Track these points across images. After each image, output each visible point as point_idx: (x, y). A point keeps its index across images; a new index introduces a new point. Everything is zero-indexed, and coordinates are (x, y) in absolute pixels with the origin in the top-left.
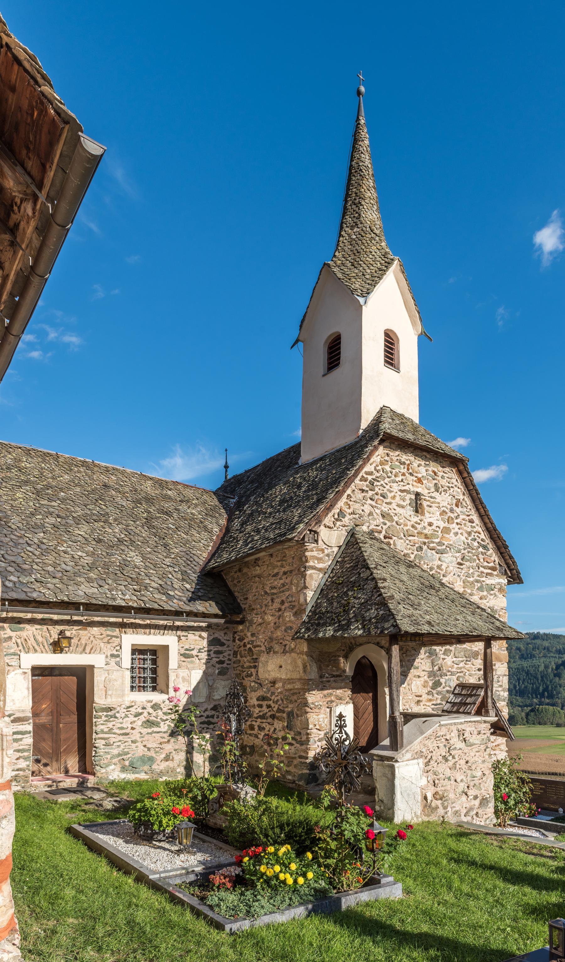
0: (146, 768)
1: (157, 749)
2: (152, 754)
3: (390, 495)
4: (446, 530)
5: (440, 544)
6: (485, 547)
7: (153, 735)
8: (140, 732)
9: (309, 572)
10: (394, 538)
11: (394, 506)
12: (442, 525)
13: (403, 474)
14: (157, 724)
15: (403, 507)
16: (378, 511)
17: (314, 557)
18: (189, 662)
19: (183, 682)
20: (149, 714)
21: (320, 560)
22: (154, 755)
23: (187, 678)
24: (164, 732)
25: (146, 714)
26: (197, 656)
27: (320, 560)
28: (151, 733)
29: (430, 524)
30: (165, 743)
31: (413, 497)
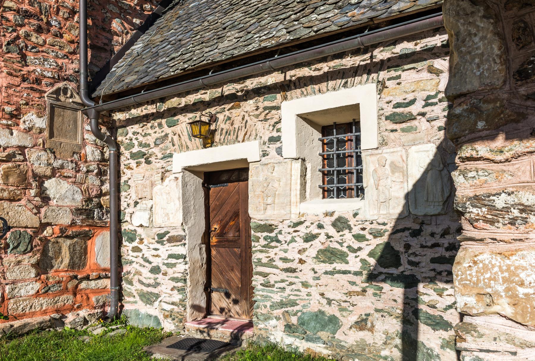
0: (324, 335)
1: (343, 304)
2: (332, 310)
7: (336, 275)
8: (313, 269)
14: (342, 257)
18: (403, 130)
19: (393, 172)
20: (328, 237)
22: (338, 314)
23: (401, 164)
24: (356, 274)
25: (322, 238)
26: (423, 114)
28: (332, 273)
30: (358, 294)
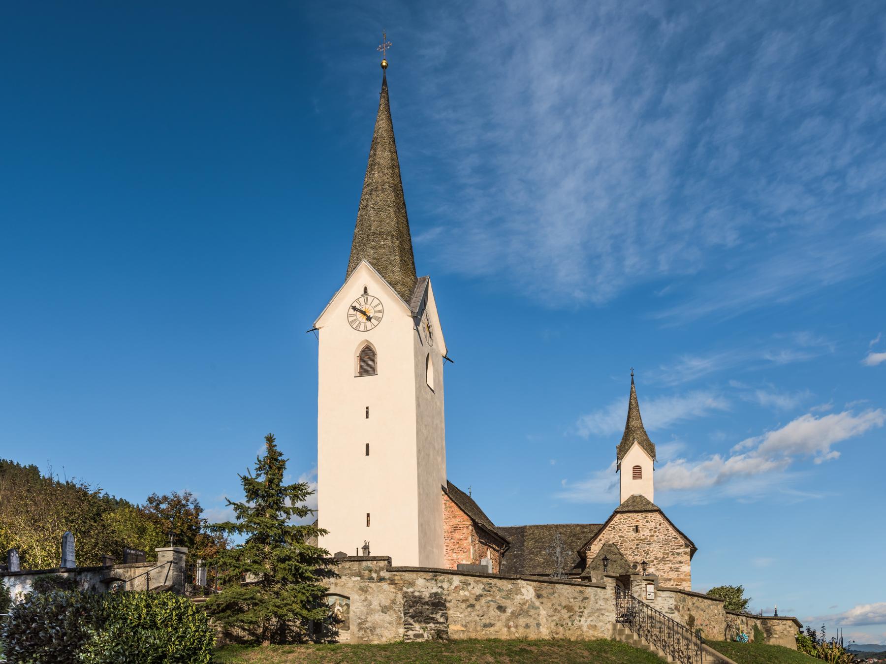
3: (622, 529)
4: (652, 536)
5: (648, 542)
6: (675, 538)
9: (588, 560)
10: (625, 543)
11: (625, 532)
12: (649, 534)
13: (630, 521)
15: (629, 532)
16: (617, 536)
17: (589, 555)
21: (591, 555)
27: (591, 555)
29: (643, 535)
31: (635, 527)
